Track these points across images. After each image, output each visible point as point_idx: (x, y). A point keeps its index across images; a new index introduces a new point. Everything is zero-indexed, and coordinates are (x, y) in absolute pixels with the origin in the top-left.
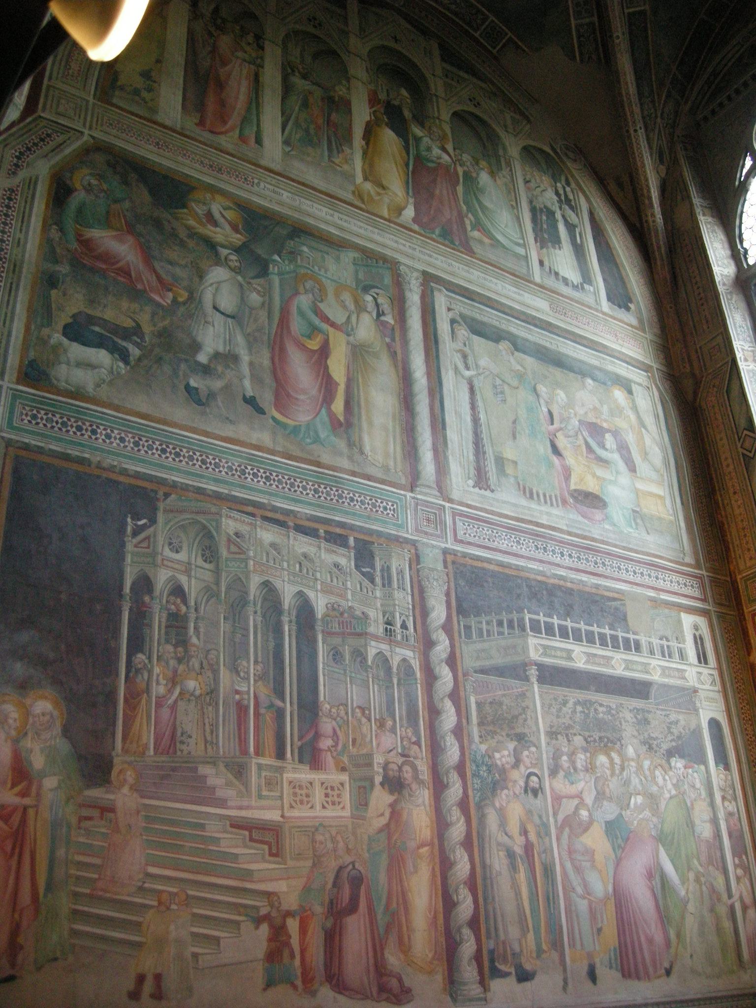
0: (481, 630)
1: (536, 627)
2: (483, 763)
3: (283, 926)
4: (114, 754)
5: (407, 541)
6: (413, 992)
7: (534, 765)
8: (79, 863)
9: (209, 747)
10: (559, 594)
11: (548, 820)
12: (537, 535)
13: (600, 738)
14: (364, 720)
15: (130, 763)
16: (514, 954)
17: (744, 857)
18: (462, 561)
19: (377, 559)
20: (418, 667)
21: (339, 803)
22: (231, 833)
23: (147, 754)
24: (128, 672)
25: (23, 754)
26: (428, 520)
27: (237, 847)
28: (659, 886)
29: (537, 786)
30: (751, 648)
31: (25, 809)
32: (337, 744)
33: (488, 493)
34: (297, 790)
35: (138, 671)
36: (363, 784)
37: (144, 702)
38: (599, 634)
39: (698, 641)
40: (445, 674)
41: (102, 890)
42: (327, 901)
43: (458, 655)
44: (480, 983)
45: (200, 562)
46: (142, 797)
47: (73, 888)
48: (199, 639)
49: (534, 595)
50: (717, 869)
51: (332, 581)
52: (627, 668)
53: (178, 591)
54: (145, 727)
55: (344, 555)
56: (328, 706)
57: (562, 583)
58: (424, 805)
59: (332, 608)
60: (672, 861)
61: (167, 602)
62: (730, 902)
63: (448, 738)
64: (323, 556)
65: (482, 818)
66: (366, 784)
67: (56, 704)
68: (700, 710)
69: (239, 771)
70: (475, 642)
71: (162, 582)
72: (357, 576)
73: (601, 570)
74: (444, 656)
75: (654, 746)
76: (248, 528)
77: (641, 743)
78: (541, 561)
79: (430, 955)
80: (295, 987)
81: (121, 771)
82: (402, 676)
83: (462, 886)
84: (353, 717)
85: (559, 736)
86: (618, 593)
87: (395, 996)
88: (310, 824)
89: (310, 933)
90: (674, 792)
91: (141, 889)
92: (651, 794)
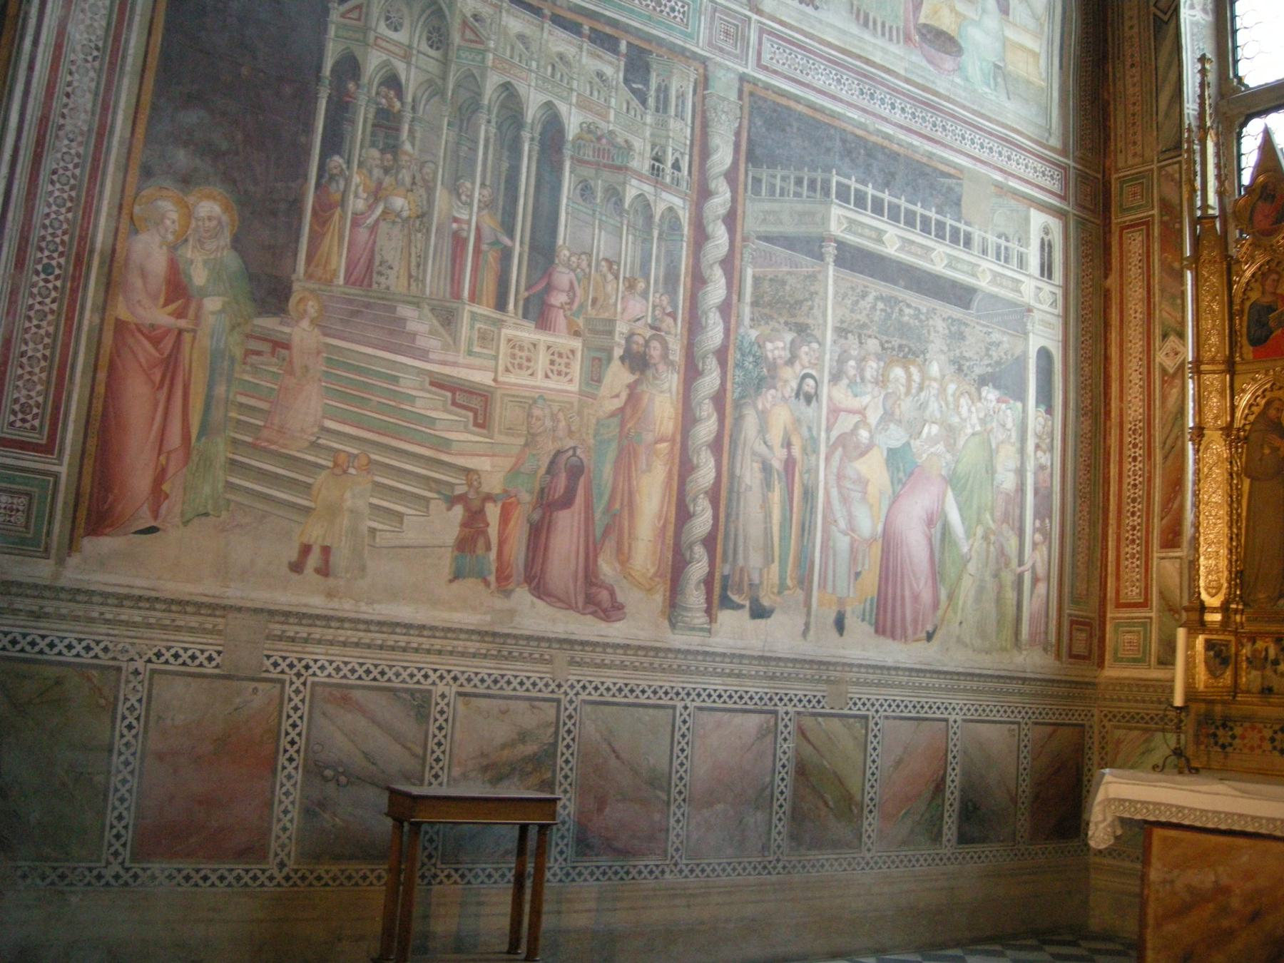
0: (773, 186)
1: (843, 194)
3: (481, 511)
4: (294, 277)
5: (695, 56)
6: (626, 610)
7: (813, 366)
8: (241, 405)
9: (413, 284)
10: (880, 156)
11: (819, 434)
12: (865, 76)
13: (900, 346)
14: (610, 277)
15: (312, 291)
16: (751, 585)
18: (762, 93)
19: (653, 75)
21: (567, 374)
22: (429, 392)
23: (335, 282)
24: (320, 176)
25: (181, 266)
26: (727, 33)
27: (436, 409)
29: (813, 391)
30: (1111, 269)
31: (180, 332)
32: (571, 303)
33: (809, 10)
34: (516, 351)
35: (332, 178)
36: (598, 354)
37: (336, 217)
38: (922, 216)
39: (1046, 247)
40: (720, 237)
41: (268, 441)
42: (537, 487)
43: (739, 212)
45: (424, 47)
46: (326, 335)
47: (232, 434)
48: (413, 145)
49: (848, 153)
50: (1013, 529)
51: (591, 94)
52: (949, 266)
53: (392, 82)
54: (335, 249)
55: (611, 63)
56: (567, 253)
57: (886, 143)
58: (670, 391)
59: (588, 129)
60: (960, 509)
61: (378, 93)
62: (1019, 570)
63: (711, 315)
64: (584, 60)
65: (739, 419)
66: (603, 355)
67: (226, 209)
69: (448, 318)
70: (763, 201)
71: (372, 67)
72: (625, 93)
73: (939, 135)
74: (722, 211)
75: (965, 368)
76: (490, 10)
78: (864, 111)
79: (652, 571)
80: (487, 584)
81: (301, 300)
82: (665, 227)
84: (597, 270)
85: (850, 335)
87: (605, 611)
88: (527, 394)
89: (512, 523)
90: (978, 428)
91: (314, 446)
92: (950, 426)
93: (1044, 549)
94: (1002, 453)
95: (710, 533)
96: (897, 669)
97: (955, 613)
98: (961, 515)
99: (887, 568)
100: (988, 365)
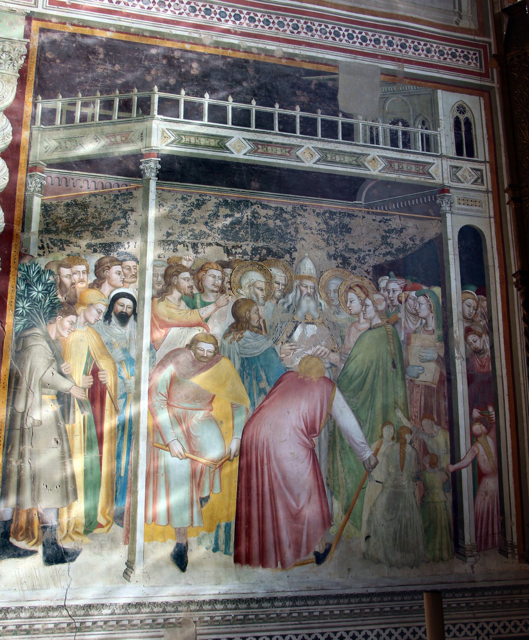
2: (39, 280)
13: (255, 250)
16: (45, 528)
17: (491, 409)
28: (325, 445)
29: (129, 311)
50: (439, 424)
60: (356, 412)
62: (452, 468)
68: (448, 216)
70: (58, 129)
73: (303, 36)
77: (329, 257)
85: (180, 247)
86: (326, 64)
90: (377, 321)
93: (490, 442)
94: (416, 342)
96: (272, 600)
97: (359, 528)
99: (249, 489)
100: (384, 255)
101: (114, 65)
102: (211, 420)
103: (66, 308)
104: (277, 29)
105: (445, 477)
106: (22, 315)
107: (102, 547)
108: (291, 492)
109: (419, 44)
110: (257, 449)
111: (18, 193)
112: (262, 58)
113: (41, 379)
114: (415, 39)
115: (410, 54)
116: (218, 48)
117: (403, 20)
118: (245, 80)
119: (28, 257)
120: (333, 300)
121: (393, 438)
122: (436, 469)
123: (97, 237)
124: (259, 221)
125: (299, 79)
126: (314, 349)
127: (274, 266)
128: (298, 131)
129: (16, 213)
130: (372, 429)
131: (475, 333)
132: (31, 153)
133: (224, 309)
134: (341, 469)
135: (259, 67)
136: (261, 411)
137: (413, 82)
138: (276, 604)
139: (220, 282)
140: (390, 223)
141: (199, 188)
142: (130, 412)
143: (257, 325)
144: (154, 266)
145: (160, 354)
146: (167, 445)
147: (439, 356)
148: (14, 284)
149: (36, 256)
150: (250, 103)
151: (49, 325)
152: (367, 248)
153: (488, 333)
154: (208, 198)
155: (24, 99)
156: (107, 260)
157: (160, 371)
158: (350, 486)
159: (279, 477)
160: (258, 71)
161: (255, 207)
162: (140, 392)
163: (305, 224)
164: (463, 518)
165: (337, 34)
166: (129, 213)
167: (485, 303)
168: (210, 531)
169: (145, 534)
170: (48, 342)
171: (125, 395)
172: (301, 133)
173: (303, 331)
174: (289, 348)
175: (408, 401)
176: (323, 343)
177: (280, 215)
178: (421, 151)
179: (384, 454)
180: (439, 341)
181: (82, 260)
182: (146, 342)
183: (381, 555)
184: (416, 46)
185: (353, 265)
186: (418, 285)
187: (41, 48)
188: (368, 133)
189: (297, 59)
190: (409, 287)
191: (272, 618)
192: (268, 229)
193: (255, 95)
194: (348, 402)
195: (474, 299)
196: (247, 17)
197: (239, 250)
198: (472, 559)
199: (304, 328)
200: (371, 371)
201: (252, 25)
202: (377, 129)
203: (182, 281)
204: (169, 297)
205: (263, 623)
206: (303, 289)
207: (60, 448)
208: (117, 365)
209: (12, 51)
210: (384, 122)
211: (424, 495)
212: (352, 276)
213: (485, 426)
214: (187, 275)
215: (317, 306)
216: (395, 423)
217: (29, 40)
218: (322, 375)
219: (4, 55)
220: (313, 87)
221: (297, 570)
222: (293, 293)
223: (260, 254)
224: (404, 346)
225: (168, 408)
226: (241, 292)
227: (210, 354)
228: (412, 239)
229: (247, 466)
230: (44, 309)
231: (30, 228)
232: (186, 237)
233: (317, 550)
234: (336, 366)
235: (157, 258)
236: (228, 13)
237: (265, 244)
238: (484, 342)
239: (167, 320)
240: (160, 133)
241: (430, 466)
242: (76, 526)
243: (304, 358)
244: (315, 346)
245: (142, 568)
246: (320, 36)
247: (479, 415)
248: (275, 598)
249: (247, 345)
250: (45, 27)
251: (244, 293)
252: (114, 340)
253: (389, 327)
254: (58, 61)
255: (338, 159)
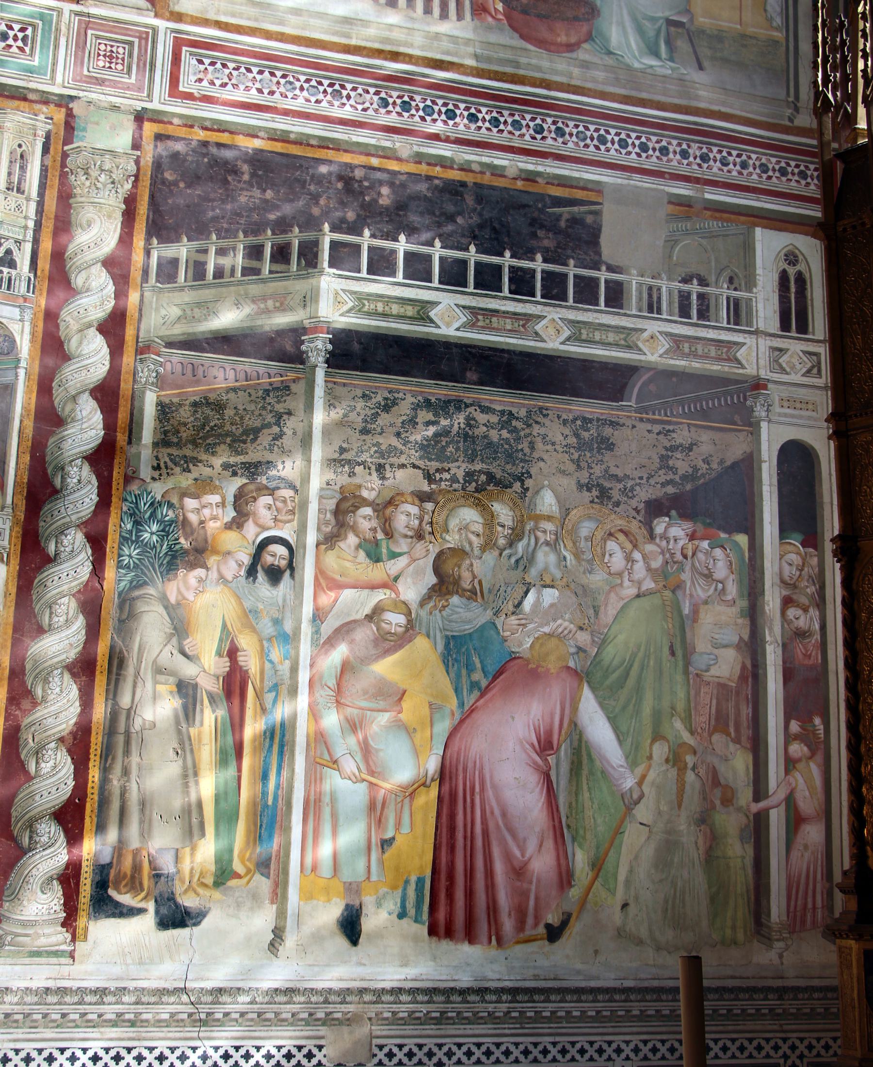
2: (153, 515)
13: (470, 475)
16: (158, 876)
17: (817, 721)
20: (27, 337)
28: (565, 767)
29: (283, 563)
44: (63, 925)
50: (737, 741)
60: (613, 721)
62: (755, 807)
63: (73, 471)
68: (764, 425)
70: (182, 289)
73: (550, 144)
77: (580, 486)
83: (53, 745)
85: (359, 469)
86: (584, 189)
90: (649, 584)
94: (707, 618)
95: (69, 802)
96: (482, 991)
97: (612, 892)
98: (616, 729)
99: (452, 829)
100: (663, 485)
101: (264, 191)
102: (399, 727)
103: (192, 558)
104: (510, 133)
105: (744, 820)
106: (129, 568)
107: (239, 905)
108: (514, 836)
109: (730, 154)
110: (465, 770)
111: (122, 384)
112: (487, 179)
113: (155, 661)
114: (724, 147)
115: (715, 170)
116: (420, 163)
117: (706, 117)
118: (460, 213)
119: (137, 481)
120: (583, 552)
121: (667, 761)
122: (731, 808)
123: (238, 453)
124: (477, 432)
125: (542, 211)
126: (553, 625)
127: (496, 500)
128: (538, 293)
129: (120, 416)
130: (637, 747)
131: (798, 606)
132: (143, 327)
133: (421, 562)
134: (588, 803)
135: (482, 193)
136: (474, 715)
137: (717, 215)
138: (488, 997)
139: (417, 522)
140: (674, 435)
141: (389, 381)
142: (283, 713)
143: (469, 587)
144: (321, 497)
145: (327, 629)
146: (335, 762)
147: (741, 638)
148: (117, 521)
149: (148, 480)
150: (467, 249)
151: (166, 583)
152: (637, 474)
153: (818, 606)
154: (401, 395)
155: (131, 243)
156: (251, 487)
157: (327, 652)
158: (601, 829)
159: (497, 812)
160: (479, 199)
161: (471, 409)
162: (297, 682)
163: (544, 437)
164: (769, 883)
165: (602, 140)
166: (285, 417)
167: (816, 559)
168: (394, 888)
169: (301, 889)
170: (166, 608)
171: (275, 688)
172: (542, 297)
173: (538, 598)
174: (517, 622)
175: (692, 705)
176: (567, 616)
177: (509, 422)
178: (725, 325)
179: (653, 783)
180: (742, 617)
181: (215, 487)
182: (307, 610)
183: (644, 933)
184: (724, 157)
185: (615, 499)
186: (714, 531)
187: (158, 165)
188: (645, 296)
189: (539, 180)
190: (698, 534)
191: (482, 1018)
192: (490, 444)
193: (475, 238)
194: (602, 705)
195: (798, 553)
196: (466, 113)
197: (446, 476)
198: (781, 944)
199: (539, 593)
200: (637, 659)
201: (473, 126)
202: (659, 289)
203: (361, 520)
204: (342, 544)
205: (469, 1024)
206: (539, 534)
207: (180, 762)
208: (265, 642)
209: (114, 170)
210: (670, 279)
211: (711, 847)
212: (613, 516)
213: (808, 747)
214: (368, 511)
215: (560, 561)
216: (670, 737)
217: (139, 153)
218: (564, 664)
219: (103, 176)
220: (563, 224)
221: (519, 950)
222: (525, 541)
223: (477, 481)
224: (688, 623)
225: (337, 707)
226: (447, 538)
227: (400, 630)
228: (706, 461)
229: (451, 794)
230: (159, 558)
231: (140, 439)
232: (368, 455)
233: (550, 921)
234: (585, 651)
235: (325, 486)
236: (436, 108)
237: (485, 466)
238: (811, 619)
239: (338, 577)
240: (331, 296)
241: (722, 803)
242: (202, 875)
243: (537, 638)
244: (555, 620)
245: (295, 938)
246: (577, 144)
247: (799, 729)
248: (486, 989)
249: (454, 616)
250: (163, 132)
251: (452, 540)
252: (261, 606)
253: (668, 593)
254: (182, 185)
255: (597, 336)
